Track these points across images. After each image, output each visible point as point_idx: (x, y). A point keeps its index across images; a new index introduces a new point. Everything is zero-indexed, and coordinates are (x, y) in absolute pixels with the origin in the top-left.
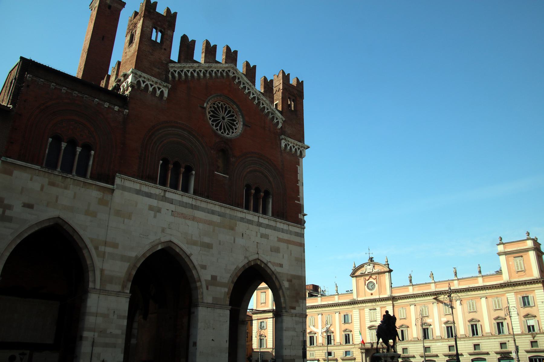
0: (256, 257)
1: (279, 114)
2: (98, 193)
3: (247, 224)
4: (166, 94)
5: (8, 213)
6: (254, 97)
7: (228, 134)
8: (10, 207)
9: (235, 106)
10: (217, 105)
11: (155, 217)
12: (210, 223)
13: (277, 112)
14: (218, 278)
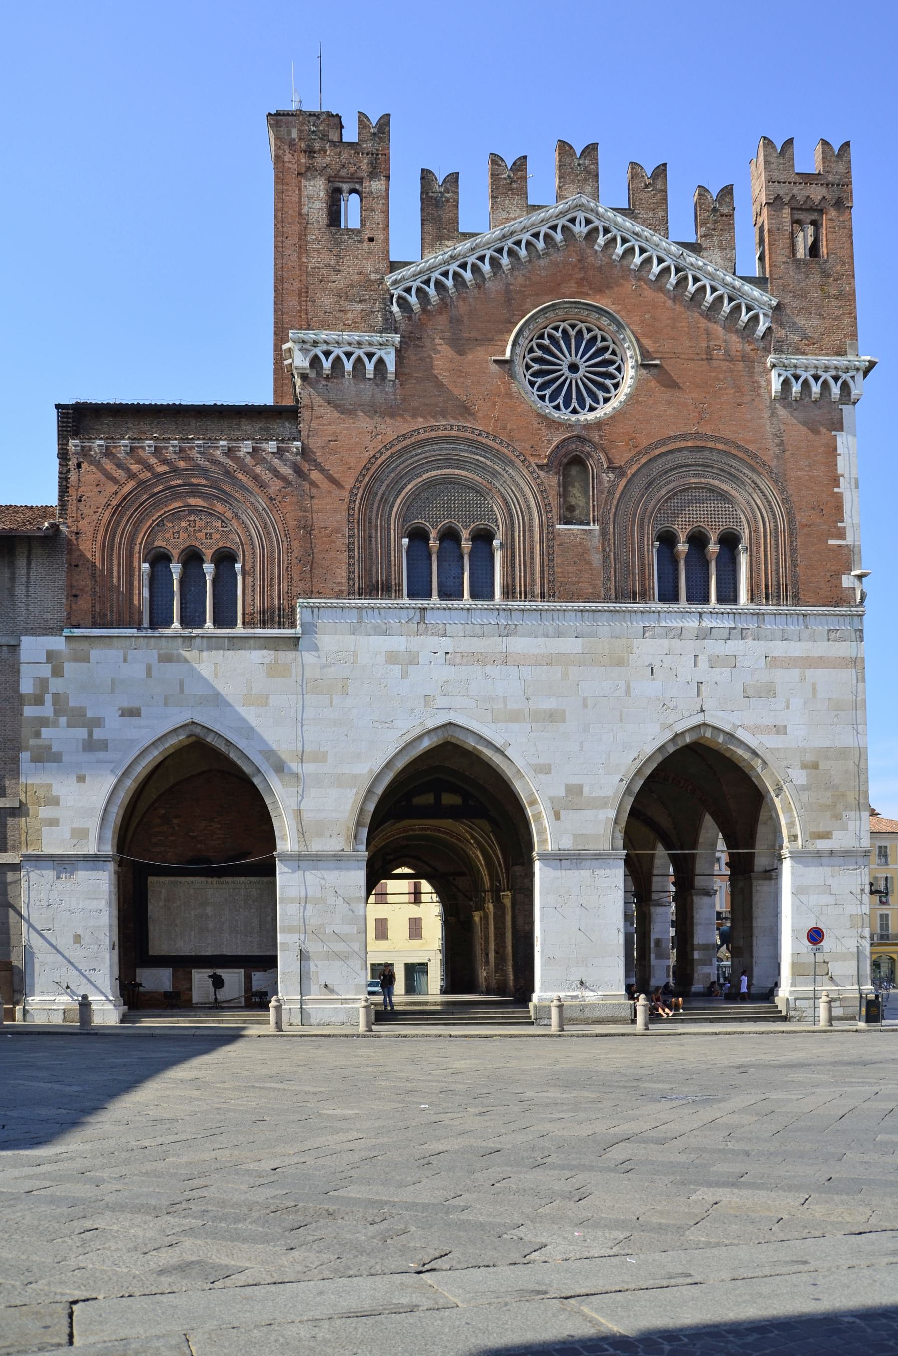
0: (697, 720)
1: (756, 293)
2: (265, 652)
3: (665, 642)
4: (391, 367)
5: (98, 734)
6: (667, 270)
7: (592, 409)
8: (98, 723)
9: (604, 321)
10: (550, 337)
11: (405, 675)
12: (551, 660)
13: (747, 288)
14: (586, 790)
